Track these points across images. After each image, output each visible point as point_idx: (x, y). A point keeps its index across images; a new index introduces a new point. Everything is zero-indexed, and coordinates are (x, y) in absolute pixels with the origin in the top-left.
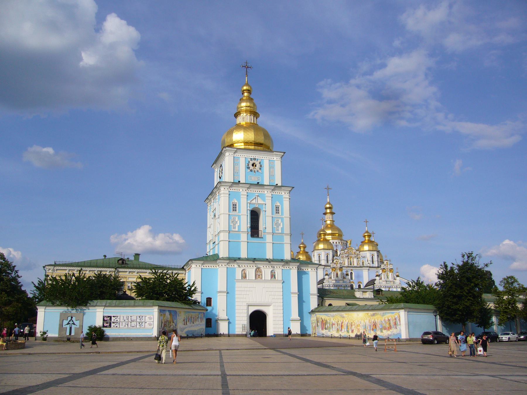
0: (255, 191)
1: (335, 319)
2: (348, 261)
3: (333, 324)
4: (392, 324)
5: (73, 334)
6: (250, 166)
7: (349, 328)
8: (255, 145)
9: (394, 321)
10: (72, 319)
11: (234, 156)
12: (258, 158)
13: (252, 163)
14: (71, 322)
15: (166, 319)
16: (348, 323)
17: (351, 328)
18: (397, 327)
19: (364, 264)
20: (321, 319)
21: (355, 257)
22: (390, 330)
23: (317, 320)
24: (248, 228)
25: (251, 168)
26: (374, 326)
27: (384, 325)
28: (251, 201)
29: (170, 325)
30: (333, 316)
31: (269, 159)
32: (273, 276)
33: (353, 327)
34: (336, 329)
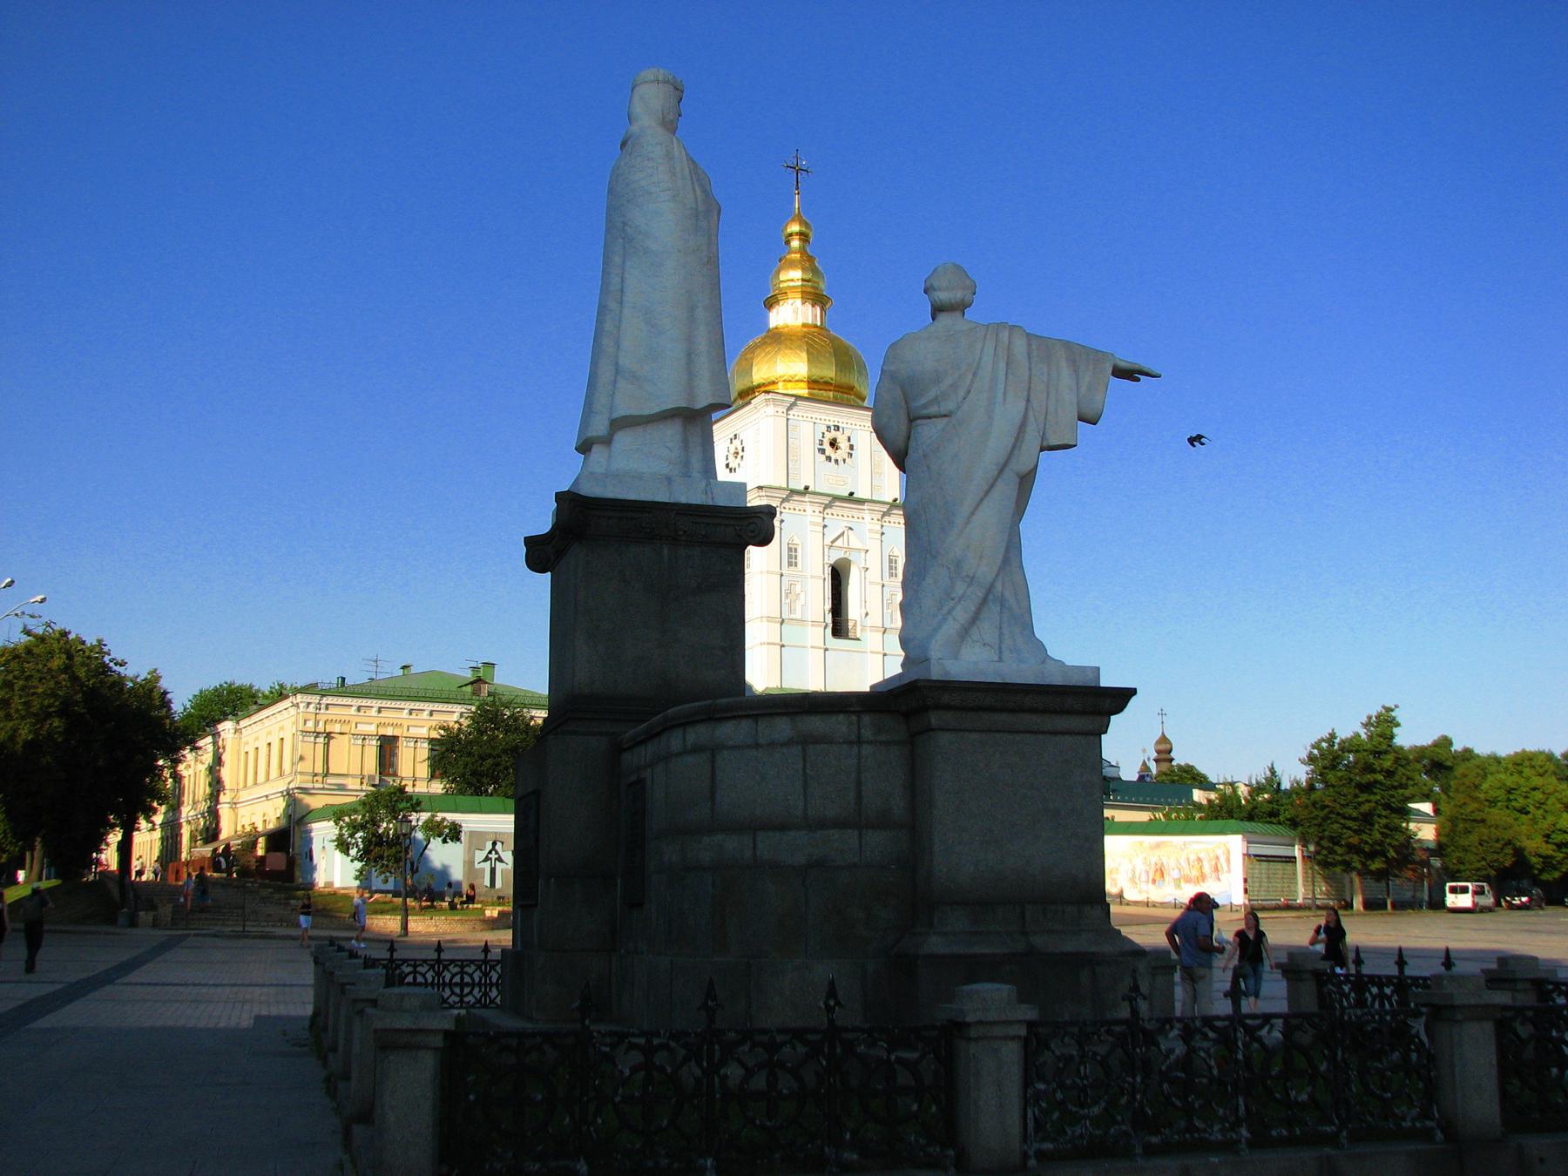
0: (839, 518)
4: (1207, 869)
5: (498, 884)
6: (826, 446)
8: (836, 389)
9: (1214, 863)
10: (497, 847)
11: (789, 417)
12: (844, 425)
14: (493, 856)
18: (1220, 877)
22: (1202, 884)
24: (827, 612)
25: (829, 451)
26: (1159, 873)
27: (1187, 871)
28: (833, 542)
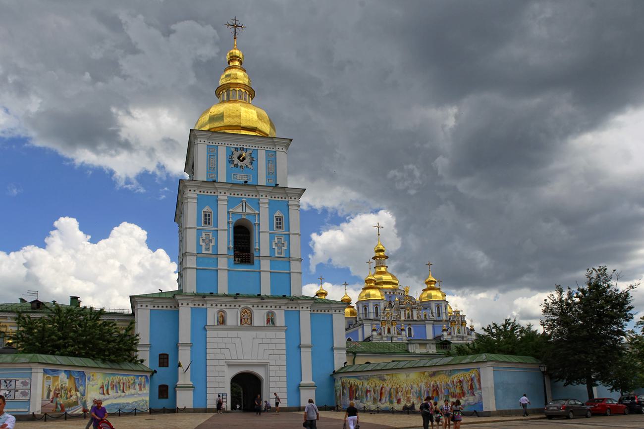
1: (370, 384)
2: (405, 314)
3: (368, 391)
7: (393, 396)
13: (238, 155)
15: (60, 385)
16: (391, 389)
17: (396, 396)
19: (427, 317)
20: (349, 383)
21: (415, 308)
23: (342, 385)
25: (236, 161)
29: (69, 395)
30: (368, 380)
31: (266, 149)
32: (271, 320)
33: (400, 394)
34: (372, 398)
